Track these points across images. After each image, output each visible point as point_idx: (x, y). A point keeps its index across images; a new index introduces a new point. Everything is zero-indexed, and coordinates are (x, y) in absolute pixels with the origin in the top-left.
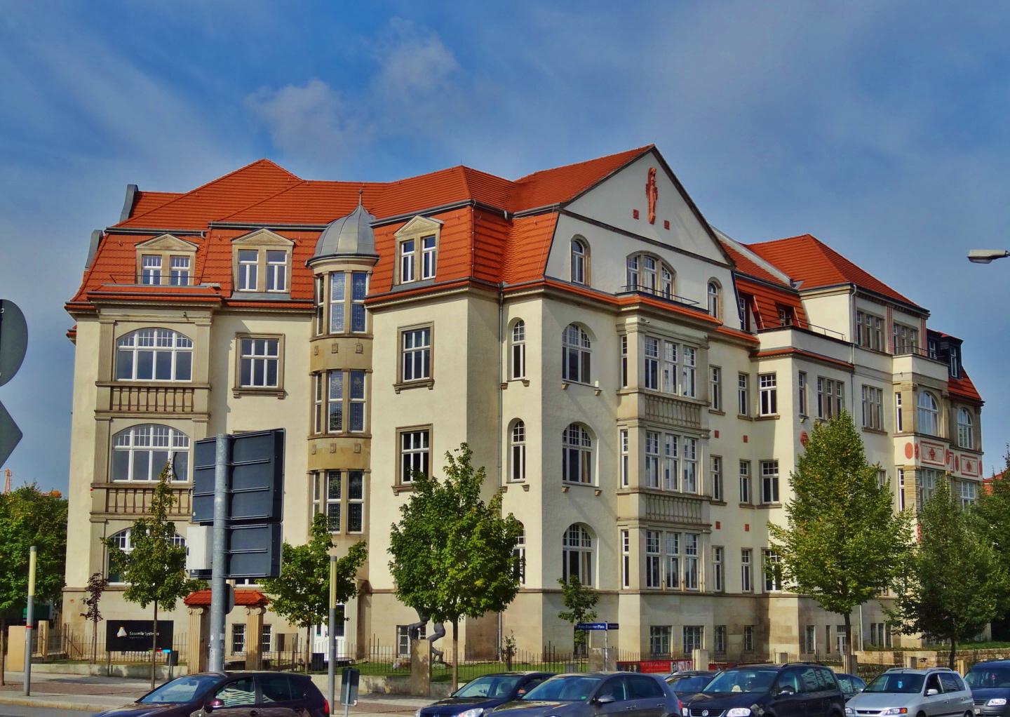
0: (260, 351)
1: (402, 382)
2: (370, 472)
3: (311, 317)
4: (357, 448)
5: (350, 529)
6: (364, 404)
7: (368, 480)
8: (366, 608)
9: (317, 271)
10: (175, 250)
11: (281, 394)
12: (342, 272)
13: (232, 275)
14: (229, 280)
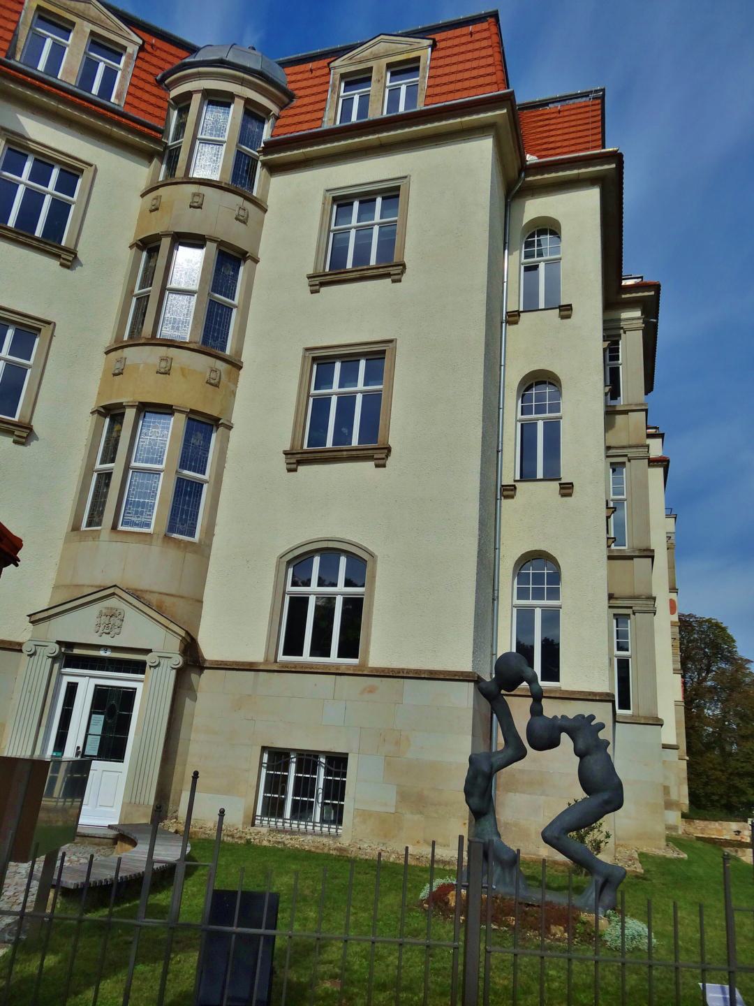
0: (40, 175)
2: (230, 428)
3: (150, 162)
4: (213, 375)
5: (172, 528)
6: (235, 311)
7: (224, 442)
8: (188, 701)
9: (174, 93)
11: (69, 259)
13: (15, 33)
14: (10, 39)
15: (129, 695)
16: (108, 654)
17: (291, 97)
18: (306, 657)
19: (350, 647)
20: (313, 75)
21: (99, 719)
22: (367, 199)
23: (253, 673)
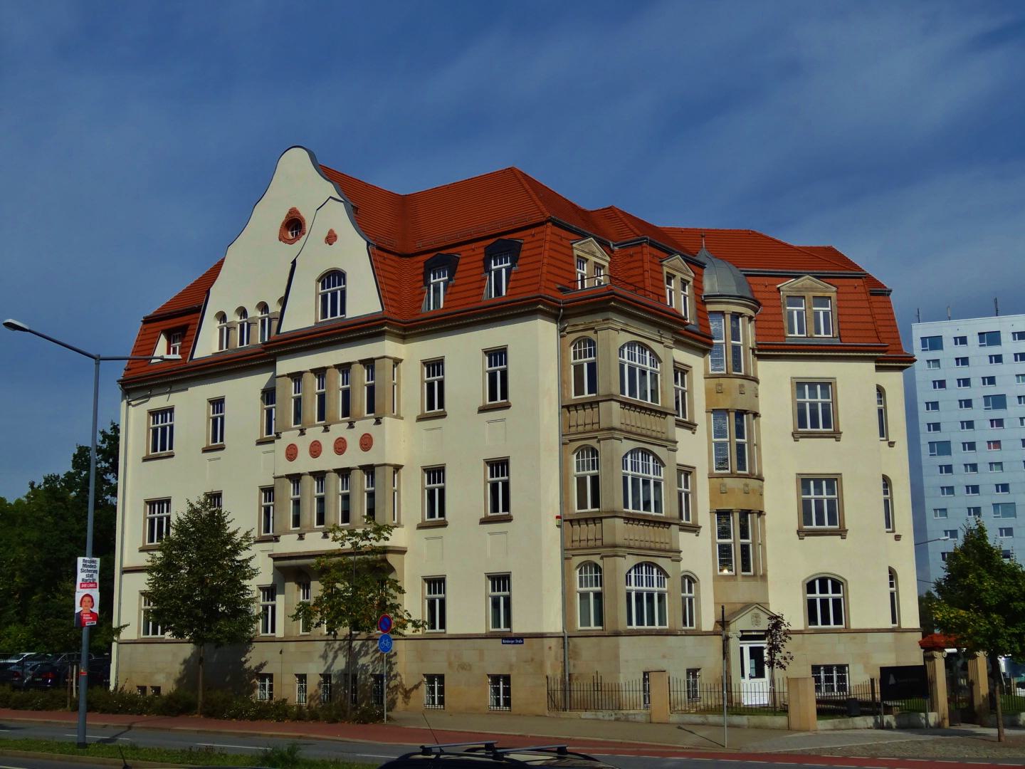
12: (723, 313)
16: (755, 633)
17: (759, 305)
18: (832, 625)
19: (838, 620)
20: (766, 289)
21: (753, 660)
22: (812, 385)
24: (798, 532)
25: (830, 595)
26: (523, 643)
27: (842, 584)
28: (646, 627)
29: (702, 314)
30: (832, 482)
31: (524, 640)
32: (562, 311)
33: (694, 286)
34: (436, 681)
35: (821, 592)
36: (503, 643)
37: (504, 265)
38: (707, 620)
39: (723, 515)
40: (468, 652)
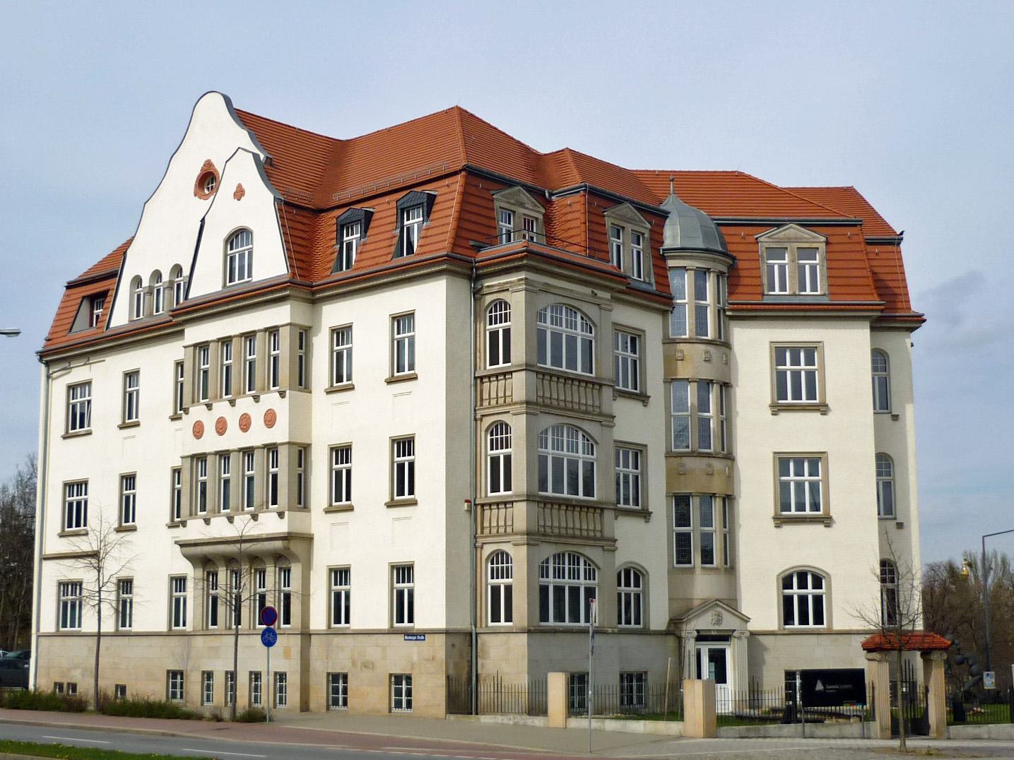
1: (393, 376)
10: (527, 208)
15: (723, 651)
19: (819, 619)
21: (713, 664)
23: (773, 637)
24: (775, 518)
25: (810, 591)
26: (424, 640)
27: (643, 575)
28: (567, 623)
29: (661, 272)
30: (815, 461)
31: (426, 635)
32: (474, 270)
33: (651, 239)
34: (338, 681)
35: (800, 587)
36: (405, 640)
37: (416, 220)
38: (658, 617)
39: (681, 501)
40: (371, 649)
